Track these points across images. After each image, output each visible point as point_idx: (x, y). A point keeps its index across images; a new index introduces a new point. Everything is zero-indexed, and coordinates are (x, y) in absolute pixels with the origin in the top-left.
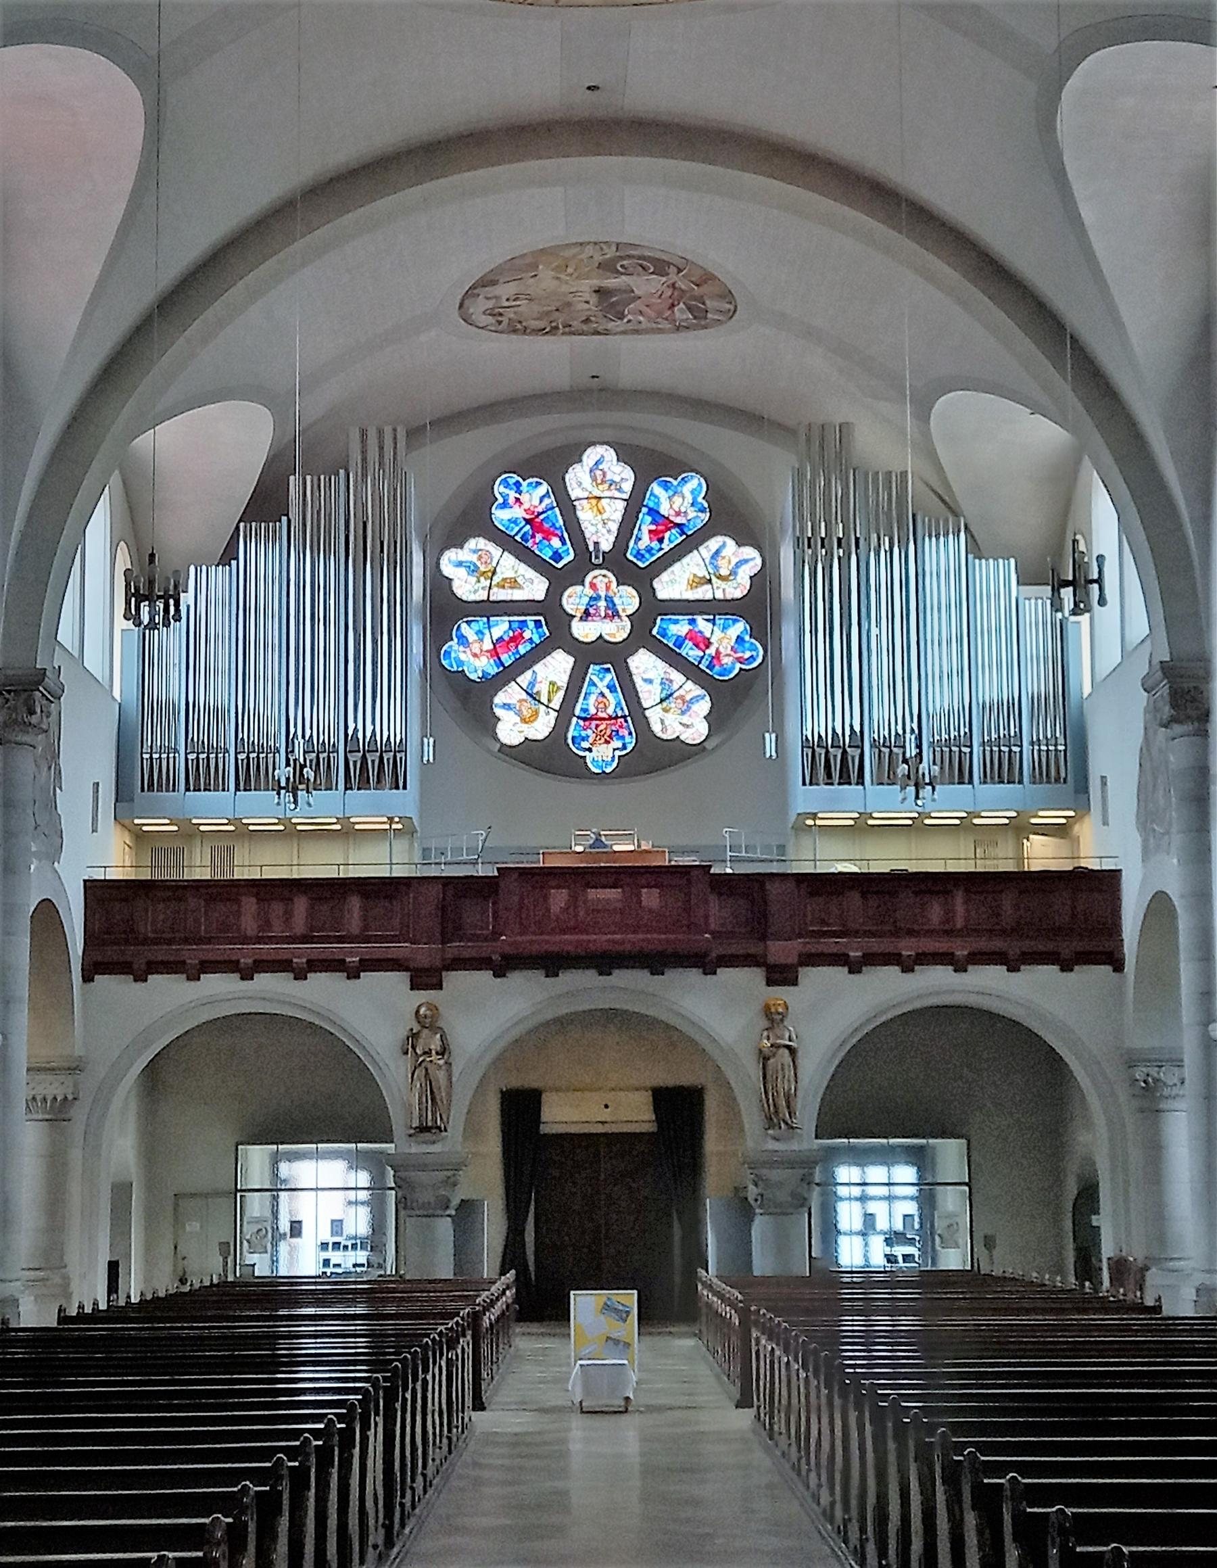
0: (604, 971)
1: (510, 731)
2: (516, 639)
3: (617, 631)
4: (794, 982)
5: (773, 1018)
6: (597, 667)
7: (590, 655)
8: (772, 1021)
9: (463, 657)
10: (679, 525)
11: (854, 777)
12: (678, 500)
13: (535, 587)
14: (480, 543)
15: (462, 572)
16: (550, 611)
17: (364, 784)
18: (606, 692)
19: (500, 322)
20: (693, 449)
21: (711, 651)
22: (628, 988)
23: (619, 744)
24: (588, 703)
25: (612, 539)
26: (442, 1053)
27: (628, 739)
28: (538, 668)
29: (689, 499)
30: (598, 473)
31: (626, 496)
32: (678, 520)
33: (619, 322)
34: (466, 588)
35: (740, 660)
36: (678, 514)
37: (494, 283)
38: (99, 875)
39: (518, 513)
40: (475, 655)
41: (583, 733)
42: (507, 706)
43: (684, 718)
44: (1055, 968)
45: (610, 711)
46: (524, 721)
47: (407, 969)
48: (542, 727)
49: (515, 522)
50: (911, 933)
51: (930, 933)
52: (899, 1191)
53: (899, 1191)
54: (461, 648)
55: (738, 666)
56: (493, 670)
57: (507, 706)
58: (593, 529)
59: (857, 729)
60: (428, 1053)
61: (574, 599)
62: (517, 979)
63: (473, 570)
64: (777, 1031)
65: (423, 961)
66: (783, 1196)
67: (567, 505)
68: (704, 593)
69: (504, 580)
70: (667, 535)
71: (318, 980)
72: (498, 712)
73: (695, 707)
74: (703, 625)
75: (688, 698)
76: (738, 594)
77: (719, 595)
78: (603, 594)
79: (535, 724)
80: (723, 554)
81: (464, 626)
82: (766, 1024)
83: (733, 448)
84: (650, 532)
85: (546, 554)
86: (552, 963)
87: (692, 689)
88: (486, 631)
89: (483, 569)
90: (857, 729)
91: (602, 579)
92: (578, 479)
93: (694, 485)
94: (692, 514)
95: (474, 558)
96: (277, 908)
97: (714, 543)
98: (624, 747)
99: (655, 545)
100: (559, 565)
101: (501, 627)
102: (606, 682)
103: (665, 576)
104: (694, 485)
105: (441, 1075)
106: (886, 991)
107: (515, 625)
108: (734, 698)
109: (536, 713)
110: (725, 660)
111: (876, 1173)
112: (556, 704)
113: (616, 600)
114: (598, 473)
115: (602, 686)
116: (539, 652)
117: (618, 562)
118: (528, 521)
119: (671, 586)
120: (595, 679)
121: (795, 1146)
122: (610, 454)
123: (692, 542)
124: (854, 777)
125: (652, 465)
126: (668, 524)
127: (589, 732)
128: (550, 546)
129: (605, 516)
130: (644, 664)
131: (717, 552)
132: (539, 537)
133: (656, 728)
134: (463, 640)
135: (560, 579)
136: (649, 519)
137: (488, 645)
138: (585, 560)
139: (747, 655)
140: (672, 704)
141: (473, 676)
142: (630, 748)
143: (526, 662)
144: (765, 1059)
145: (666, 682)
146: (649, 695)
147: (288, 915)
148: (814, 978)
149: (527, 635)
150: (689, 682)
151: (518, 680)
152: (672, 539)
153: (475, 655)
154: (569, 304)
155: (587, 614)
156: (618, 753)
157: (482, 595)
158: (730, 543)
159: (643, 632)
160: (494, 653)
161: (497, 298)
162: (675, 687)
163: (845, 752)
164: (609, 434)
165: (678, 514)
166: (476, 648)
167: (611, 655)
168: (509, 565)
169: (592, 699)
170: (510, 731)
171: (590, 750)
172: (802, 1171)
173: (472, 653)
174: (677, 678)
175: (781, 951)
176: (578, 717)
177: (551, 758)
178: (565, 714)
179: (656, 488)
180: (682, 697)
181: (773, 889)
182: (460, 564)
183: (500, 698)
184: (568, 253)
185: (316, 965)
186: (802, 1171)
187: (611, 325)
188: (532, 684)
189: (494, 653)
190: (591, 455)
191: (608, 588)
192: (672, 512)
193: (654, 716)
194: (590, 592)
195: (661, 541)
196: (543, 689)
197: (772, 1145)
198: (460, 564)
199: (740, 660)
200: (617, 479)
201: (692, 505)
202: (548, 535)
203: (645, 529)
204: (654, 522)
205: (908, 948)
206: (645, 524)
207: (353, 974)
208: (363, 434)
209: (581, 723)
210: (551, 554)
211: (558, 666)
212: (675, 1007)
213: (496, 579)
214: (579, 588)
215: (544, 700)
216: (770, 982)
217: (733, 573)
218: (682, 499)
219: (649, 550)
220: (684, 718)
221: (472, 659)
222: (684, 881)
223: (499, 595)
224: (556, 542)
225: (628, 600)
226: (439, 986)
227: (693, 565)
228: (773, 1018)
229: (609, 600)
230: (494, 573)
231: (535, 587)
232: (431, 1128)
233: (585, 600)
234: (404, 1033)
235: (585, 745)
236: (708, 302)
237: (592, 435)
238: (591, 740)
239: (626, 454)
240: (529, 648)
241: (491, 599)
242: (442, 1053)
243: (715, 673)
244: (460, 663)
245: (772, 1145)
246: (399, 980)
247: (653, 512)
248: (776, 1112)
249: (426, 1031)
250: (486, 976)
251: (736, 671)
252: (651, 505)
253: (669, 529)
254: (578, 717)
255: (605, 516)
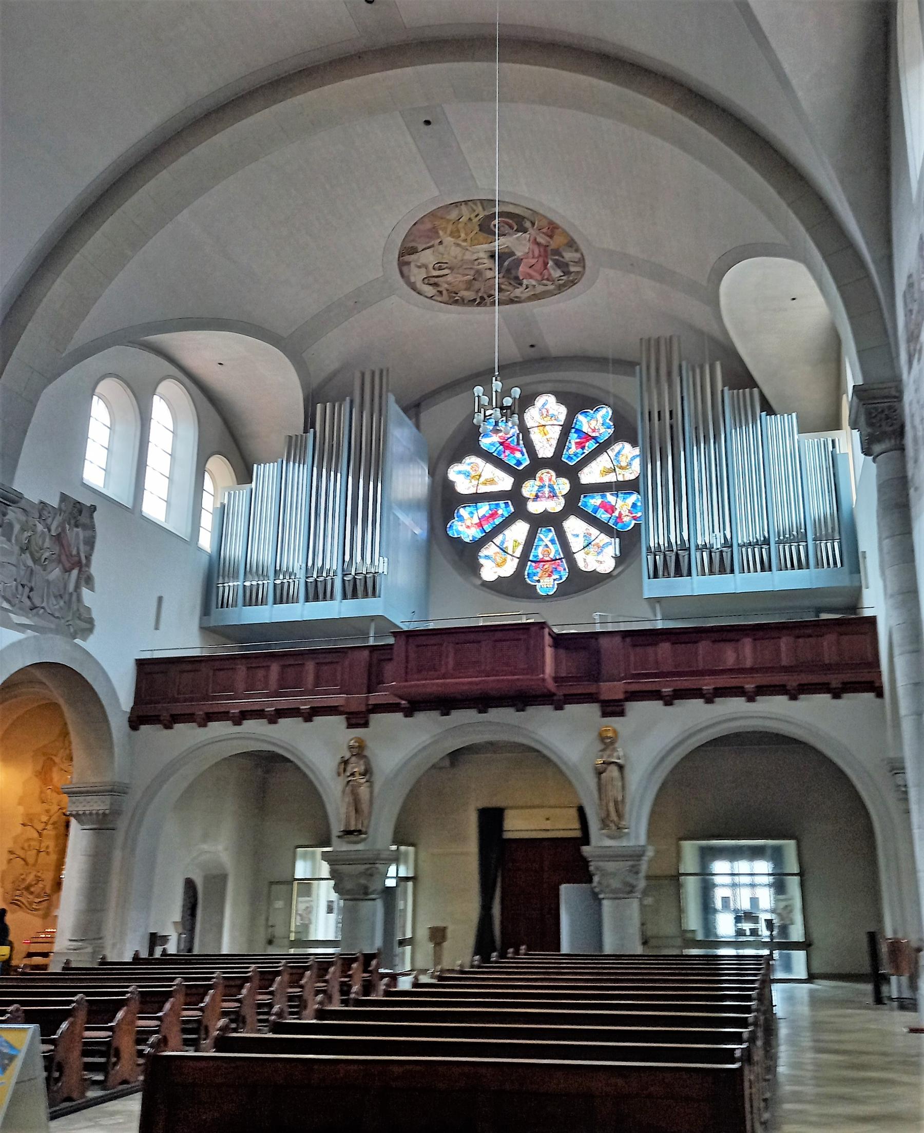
0: (482, 711)
1: (489, 573)
2: (493, 515)
3: (556, 506)
4: (621, 714)
5: (607, 742)
6: (544, 529)
7: (539, 522)
8: (605, 744)
9: (460, 529)
10: (594, 438)
11: (685, 571)
12: (593, 423)
13: (505, 482)
14: (472, 459)
15: (462, 476)
16: (515, 496)
17: (355, 595)
18: (549, 544)
19: (441, 292)
20: (599, 388)
21: (616, 514)
22: (501, 723)
23: (556, 576)
24: (538, 552)
25: (553, 450)
26: (364, 774)
27: (563, 573)
28: (507, 532)
29: (601, 421)
30: (544, 411)
31: (562, 423)
32: (594, 435)
33: (521, 289)
34: (464, 486)
35: (635, 518)
36: (594, 431)
37: (413, 251)
38: (147, 655)
39: (495, 439)
40: (468, 527)
41: (535, 571)
42: (487, 557)
43: (599, 556)
44: (827, 696)
45: (552, 556)
46: (498, 565)
47: (341, 713)
48: (509, 569)
49: (493, 444)
50: (713, 673)
51: (723, 672)
52: (758, 880)
53: (758, 880)
54: (460, 523)
55: (634, 522)
56: (478, 534)
57: (487, 557)
58: (541, 445)
59: (686, 538)
60: (353, 774)
61: (529, 489)
62: (421, 717)
63: (467, 475)
64: (608, 752)
65: (354, 708)
66: (615, 884)
67: (524, 431)
68: (611, 478)
69: (486, 480)
70: (587, 444)
71: (285, 723)
72: (482, 561)
73: (605, 550)
74: (610, 498)
75: (601, 544)
76: (633, 477)
77: (621, 479)
78: (547, 484)
79: (504, 567)
80: (623, 452)
81: (462, 511)
82: (602, 747)
83: (627, 387)
84: (576, 443)
85: (512, 463)
86: (445, 704)
87: (604, 538)
88: (475, 512)
89: (473, 474)
90: (686, 538)
91: (547, 475)
92: (532, 416)
93: (605, 413)
94: (602, 430)
95: (468, 468)
96: (261, 673)
97: (617, 447)
98: (561, 579)
99: (580, 451)
100: (521, 468)
101: (484, 508)
102: (549, 539)
103: (586, 470)
104: (605, 413)
105: (364, 791)
106: (695, 719)
107: (493, 507)
108: (629, 541)
109: (505, 561)
110: (626, 519)
111: (743, 866)
112: (518, 553)
113: (556, 487)
114: (544, 411)
115: (547, 541)
116: (508, 522)
117: (557, 464)
118: (501, 444)
119: (589, 476)
120: (541, 536)
121: (625, 843)
122: (551, 399)
123: (603, 447)
124: (685, 571)
125: (578, 403)
126: (588, 437)
127: (538, 570)
128: (515, 457)
129: (548, 436)
130: (574, 526)
131: (619, 453)
132: (507, 452)
133: (581, 565)
134: (461, 518)
135: (521, 477)
136: (576, 435)
137: (476, 520)
138: (537, 464)
139: (639, 514)
140: (591, 549)
141: (467, 540)
142: (564, 579)
143: (498, 530)
144: (599, 773)
145: (587, 536)
146: (576, 544)
147: (266, 677)
148: (636, 709)
149: (500, 512)
150: (602, 535)
151: (494, 540)
152: (591, 446)
153: (468, 527)
154: (479, 273)
155: (537, 496)
156: (556, 582)
157: (473, 491)
158: (627, 446)
159: (572, 506)
160: (480, 525)
161: (425, 266)
162: (593, 538)
163: (677, 555)
164: (549, 386)
165: (594, 431)
166: (468, 523)
167: (552, 521)
168: (489, 470)
169: (540, 549)
170: (489, 573)
171: (538, 581)
172: (630, 863)
173: (466, 526)
174: (594, 532)
175: (612, 689)
176: (532, 561)
177: (516, 586)
178: (524, 559)
179: (580, 417)
180: (597, 545)
181: (604, 642)
182: (460, 472)
183: (484, 552)
184: (454, 215)
185: (281, 713)
186: (630, 863)
187: (518, 292)
188: (503, 542)
189: (480, 525)
190: (540, 401)
191: (550, 480)
192: (590, 430)
193: (580, 558)
194: (538, 483)
195: (583, 448)
196: (509, 545)
197: (608, 843)
198: (460, 472)
199: (635, 518)
200: (556, 413)
201: (603, 424)
202: (513, 450)
203: (573, 442)
204: (579, 437)
205: (708, 685)
206: (573, 438)
207: (309, 716)
208: (363, 374)
209: (533, 564)
210: (515, 462)
211: (519, 530)
212: (533, 735)
213: (482, 480)
214: (531, 482)
215: (510, 551)
216: (605, 714)
217: (629, 464)
218: (598, 422)
219: (576, 455)
220: (599, 556)
221: (467, 530)
222: (525, 636)
223: (483, 489)
224: (518, 455)
225: (564, 486)
226: (366, 725)
227: (603, 461)
228: (607, 742)
229: (551, 487)
230: (480, 476)
231: (505, 482)
232: (354, 831)
233: (536, 488)
234: (338, 760)
235: (536, 578)
236: (564, 254)
237: (540, 388)
238: (539, 575)
239: (561, 398)
240: (501, 520)
241: (479, 492)
242: (364, 774)
243: (619, 527)
244: (458, 532)
245: (608, 843)
246: (338, 721)
247: (578, 431)
248: (608, 815)
249: (354, 759)
250: (399, 716)
251: (632, 526)
252: (577, 427)
253: (588, 441)
254: (532, 561)
255: (548, 436)
